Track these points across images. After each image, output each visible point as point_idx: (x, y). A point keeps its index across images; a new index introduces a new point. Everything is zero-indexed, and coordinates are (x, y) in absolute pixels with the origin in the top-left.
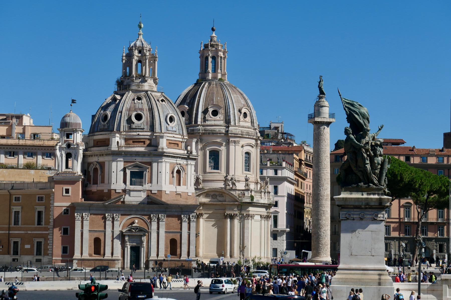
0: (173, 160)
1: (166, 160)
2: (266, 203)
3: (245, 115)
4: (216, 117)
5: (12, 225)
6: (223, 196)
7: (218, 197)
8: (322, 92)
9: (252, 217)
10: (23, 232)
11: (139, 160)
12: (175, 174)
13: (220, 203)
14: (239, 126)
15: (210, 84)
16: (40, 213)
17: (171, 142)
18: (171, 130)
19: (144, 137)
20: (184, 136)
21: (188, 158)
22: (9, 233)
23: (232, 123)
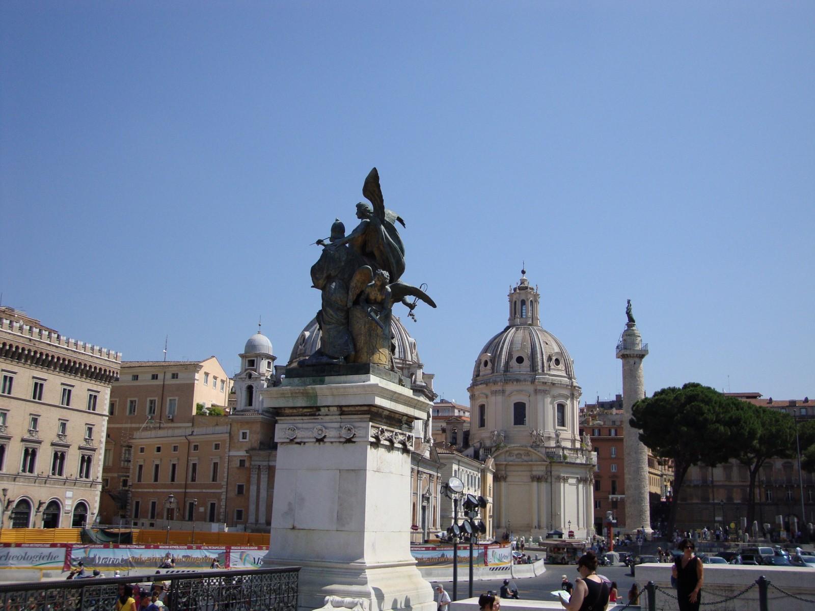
2: (584, 462)
3: (557, 362)
4: (521, 364)
5: (189, 482)
6: (529, 455)
9: (565, 480)
10: (198, 491)
13: (525, 463)
14: (549, 375)
15: (517, 329)
16: (216, 465)
20: (406, 361)
22: (185, 492)
23: (540, 371)
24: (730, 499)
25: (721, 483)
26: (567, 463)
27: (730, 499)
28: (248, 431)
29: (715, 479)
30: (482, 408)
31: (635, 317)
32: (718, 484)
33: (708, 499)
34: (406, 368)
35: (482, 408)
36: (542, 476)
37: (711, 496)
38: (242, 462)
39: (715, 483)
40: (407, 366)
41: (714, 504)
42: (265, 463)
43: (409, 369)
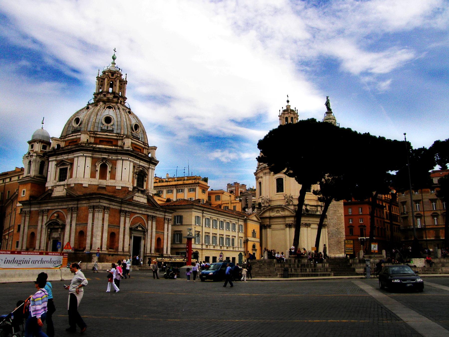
0: (98, 155)
1: (85, 155)
7: (280, 212)
8: (329, 109)
11: (65, 157)
12: (98, 169)
17: (102, 139)
18: (106, 128)
19: (75, 137)
21: (116, 152)
24: (437, 237)
25: (431, 227)
26: (309, 214)
27: (437, 237)
28: (25, 190)
29: (426, 224)
30: (260, 183)
31: (331, 108)
32: (429, 227)
33: (423, 237)
34: (120, 139)
35: (260, 183)
36: (292, 224)
37: (424, 236)
38: (21, 209)
39: (427, 227)
40: (121, 138)
41: (427, 241)
42: (29, 209)
43: (122, 140)
